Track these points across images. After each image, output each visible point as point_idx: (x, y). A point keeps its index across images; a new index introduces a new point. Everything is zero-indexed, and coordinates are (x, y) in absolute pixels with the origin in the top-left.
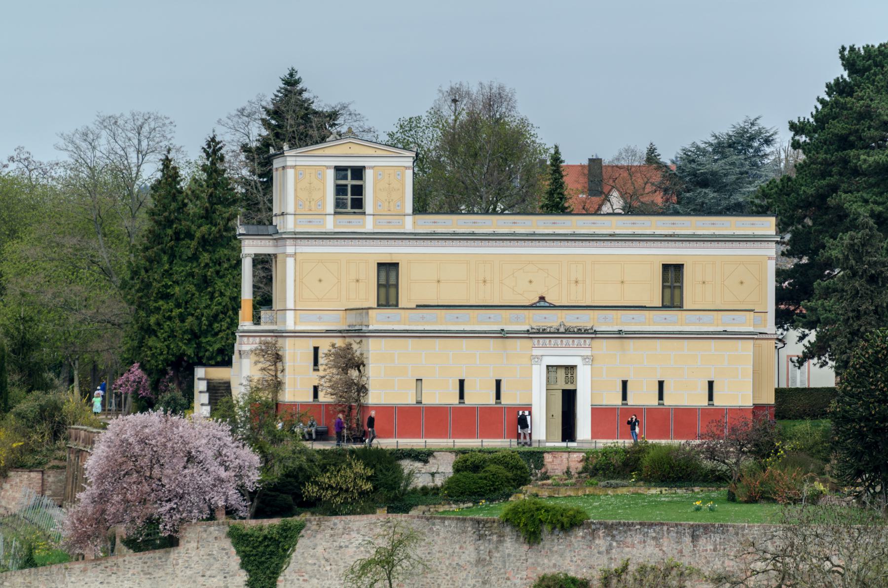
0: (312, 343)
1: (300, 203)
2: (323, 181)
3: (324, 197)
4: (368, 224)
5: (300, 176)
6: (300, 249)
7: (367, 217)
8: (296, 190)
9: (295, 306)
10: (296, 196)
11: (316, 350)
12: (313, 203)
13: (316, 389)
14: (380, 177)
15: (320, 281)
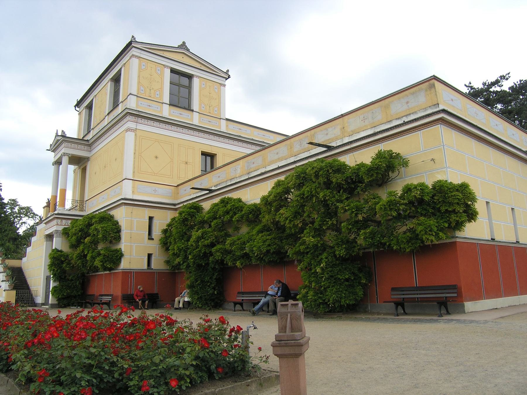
0: (148, 213)
1: (142, 88)
2: (162, 75)
3: (161, 89)
4: (195, 120)
5: (143, 67)
6: (140, 127)
7: (194, 112)
8: (139, 77)
9: (134, 176)
10: (139, 82)
11: (151, 219)
12: (152, 91)
13: (150, 256)
14: (203, 86)
15: (156, 157)
